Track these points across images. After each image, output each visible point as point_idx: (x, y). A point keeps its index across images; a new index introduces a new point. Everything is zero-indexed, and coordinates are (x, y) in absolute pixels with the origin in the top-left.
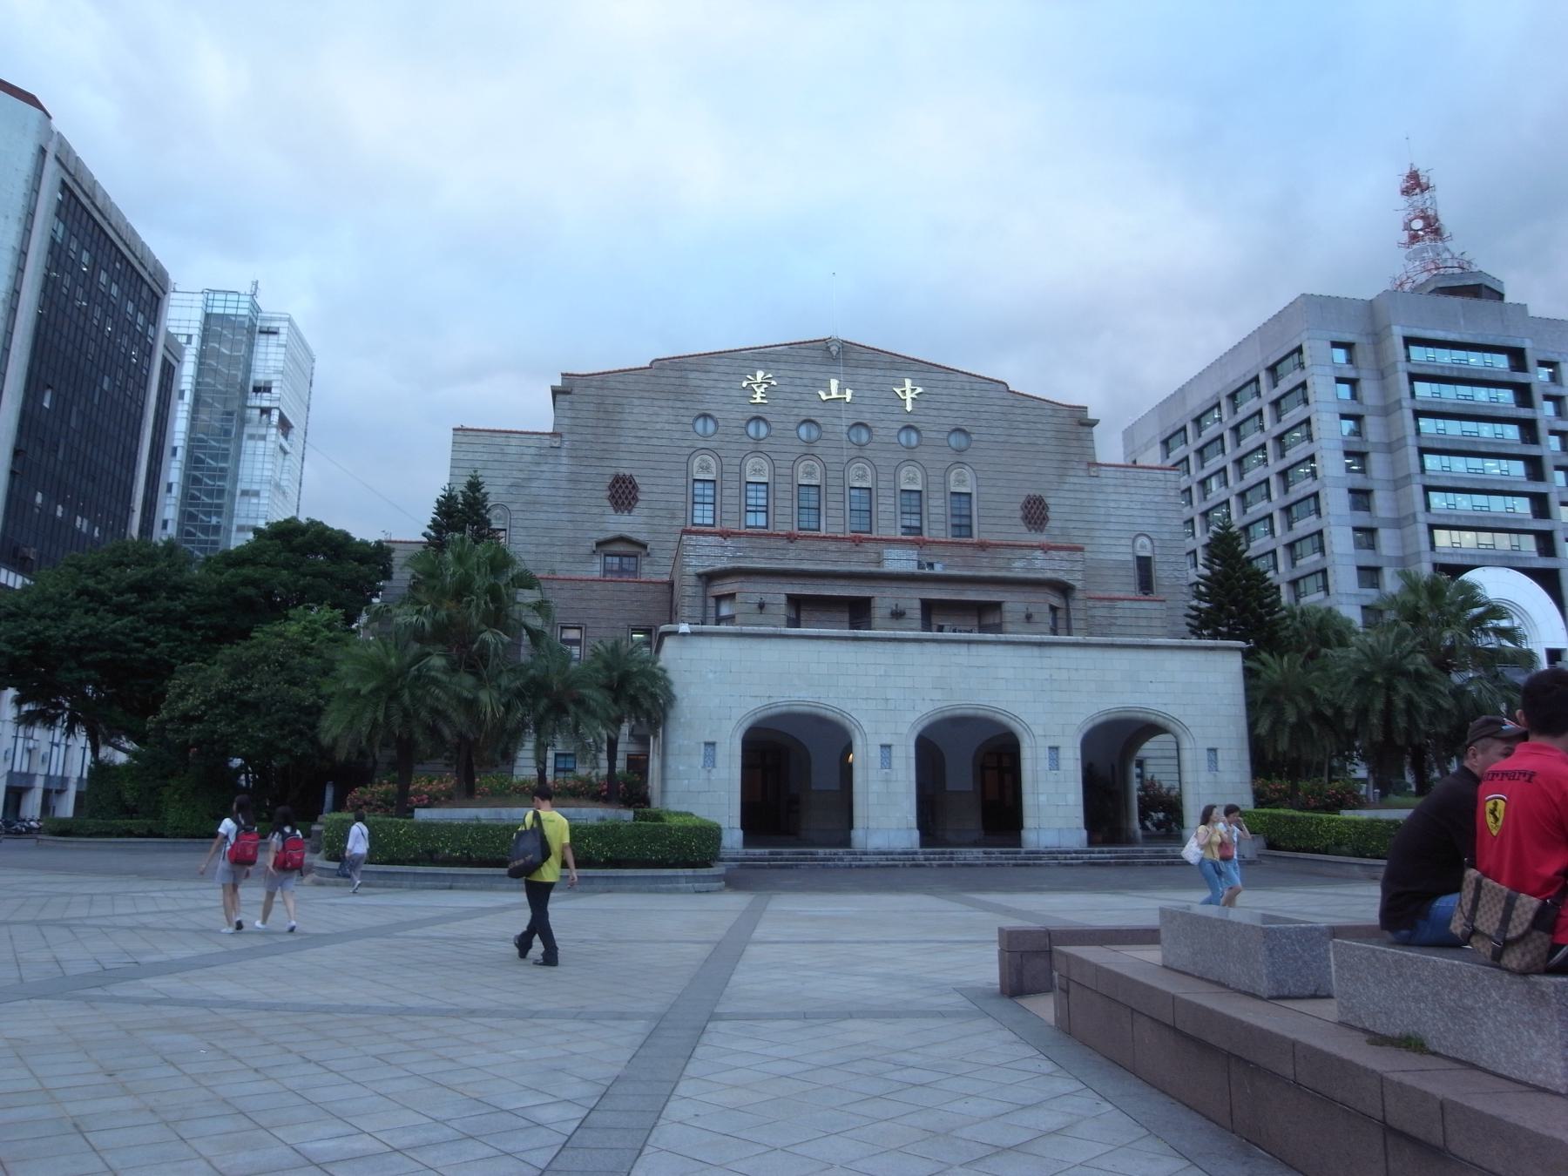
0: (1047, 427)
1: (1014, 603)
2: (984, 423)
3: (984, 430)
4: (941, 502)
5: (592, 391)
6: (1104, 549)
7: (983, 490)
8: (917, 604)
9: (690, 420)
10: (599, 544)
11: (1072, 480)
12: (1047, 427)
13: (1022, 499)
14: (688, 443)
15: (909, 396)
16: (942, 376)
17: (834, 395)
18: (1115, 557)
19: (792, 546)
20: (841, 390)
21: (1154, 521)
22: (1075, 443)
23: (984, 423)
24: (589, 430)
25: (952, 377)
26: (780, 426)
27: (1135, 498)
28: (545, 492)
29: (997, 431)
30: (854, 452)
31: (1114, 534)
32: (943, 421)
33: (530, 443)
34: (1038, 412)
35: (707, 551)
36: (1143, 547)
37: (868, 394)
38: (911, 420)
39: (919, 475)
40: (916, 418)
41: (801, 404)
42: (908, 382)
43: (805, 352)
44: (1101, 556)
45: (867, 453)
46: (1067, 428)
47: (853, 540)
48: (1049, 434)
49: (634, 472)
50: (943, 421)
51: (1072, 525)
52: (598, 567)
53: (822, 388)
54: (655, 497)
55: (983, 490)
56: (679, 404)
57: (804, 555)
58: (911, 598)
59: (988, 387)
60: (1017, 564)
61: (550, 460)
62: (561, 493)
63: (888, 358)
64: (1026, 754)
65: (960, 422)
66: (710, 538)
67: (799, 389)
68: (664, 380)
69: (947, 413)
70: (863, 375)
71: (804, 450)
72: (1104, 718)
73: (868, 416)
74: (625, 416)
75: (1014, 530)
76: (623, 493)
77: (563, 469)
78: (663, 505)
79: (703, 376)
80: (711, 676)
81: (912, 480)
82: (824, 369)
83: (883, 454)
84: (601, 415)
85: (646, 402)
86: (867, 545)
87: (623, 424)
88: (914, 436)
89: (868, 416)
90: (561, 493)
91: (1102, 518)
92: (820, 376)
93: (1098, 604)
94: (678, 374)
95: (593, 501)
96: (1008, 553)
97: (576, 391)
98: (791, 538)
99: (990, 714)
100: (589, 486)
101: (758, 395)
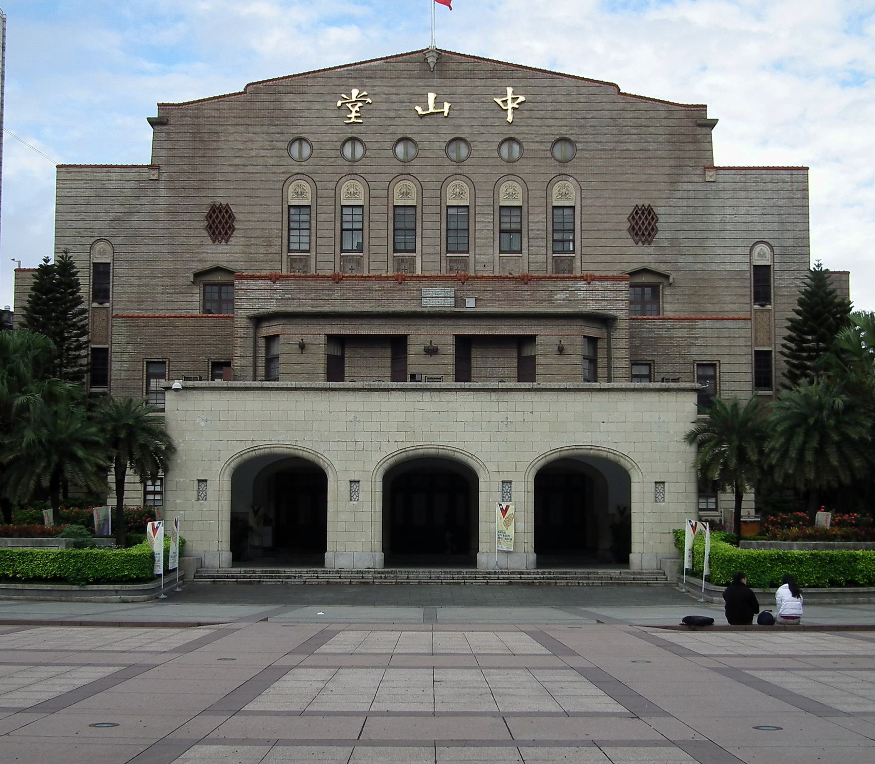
0: (661, 131)
1: (547, 336)
2: (590, 130)
3: (590, 138)
4: (542, 217)
5: (188, 120)
6: (718, 259)
7: (584, 202)
8: (451, 340)
9: (285, 145)
10: (197, 275)
11: (685, 186)
12: (661, 131)
13: (630, 210)
14: (283, 169)
15: (510, 105)
16: (547, 82)
17: (431, 110)
19: (337, 287)
20: (438, 103)
21: (776, 226)
22: (690, 146)
23: (590, 130)
24: (186, 161)
25: (557, 82)
26: (377, 146)
27: (755, 202)
28: (146, 225)
30: (451, 170)
31: (729, 243)
32: (547, 130)
33: (131, 176)
34: (652, 114)
35: (257, 294)
37: (466, 106)
38: (512, 132)
40: (518, 130)
41: (398, 121)
42: (510, 90)
43: (402, 66)
44: (714, 267)
45: (465, 170)
46: (682, 130)
47: (396, 278)
49: (230, 201)
50: (547, 130)
51: (681, 235)
52: (197, 297)
54: (251, 225)
55: (584, 202)
56: (273, 129)
57: (350, 295)
58: (445, 336)
59: (596, 90)
60: (560, 296)
61: (149, 193)
62: (160, 225)
63: (489, 66)
64: (482, 486)
65: (564, 131)
66: (260, 283)
67: (395, 106)
68: (258, 105)
69: (551, 122)
70: (462, 86)
71: (400, 170)
72: (556, 455)
73: (467, 130)
74: (221, 145)
75: (619, 243)
76: (220, 223)
77: (161, 201)
78: (258, 233)
79: (298, 98)
80: (203, 424)
81: (511, 196)
82: (420, 82)
83: (481, 170)
84: (198, 145)
85: (241, 129)
86: (410, 283)
87: (219, 153)
88: (516, 147)
89: (467, 130)
90: (160, 225)
91: (717, 227)
92: (418, 91)
94: (272, 97)
95: (192, 232)
96: (550, 286)
97: (172, 121)
98: (337, 279)
99: (450, 453)
100: (187, 217)
101: (353, 115)
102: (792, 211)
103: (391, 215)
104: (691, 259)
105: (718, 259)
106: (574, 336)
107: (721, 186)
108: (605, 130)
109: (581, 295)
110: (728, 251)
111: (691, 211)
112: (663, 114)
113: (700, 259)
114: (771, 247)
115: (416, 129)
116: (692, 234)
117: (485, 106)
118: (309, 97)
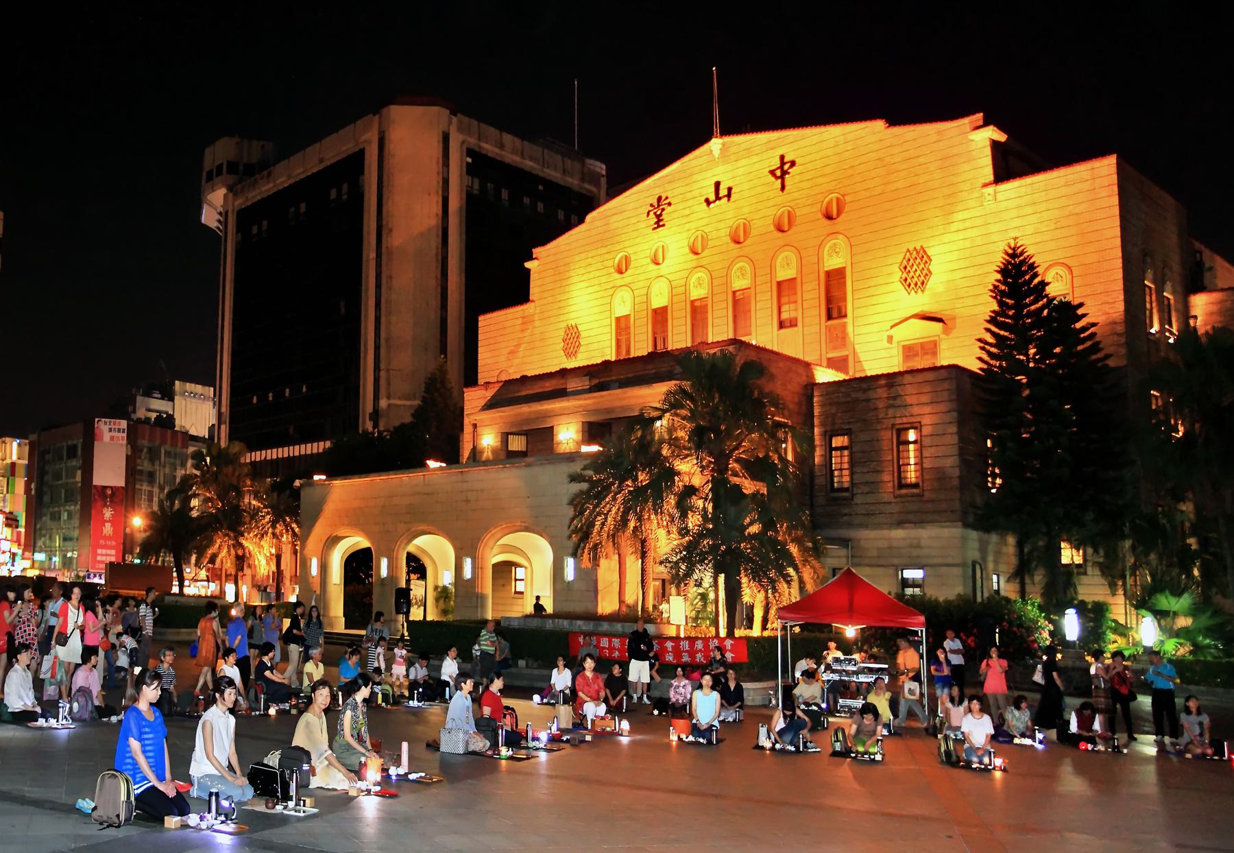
11: (961, 216)
41: (693, 217)
49: (577, 321)
68: (594, 232)
69: (821, 180)
114: (1069, 268)
115: (705, 221)
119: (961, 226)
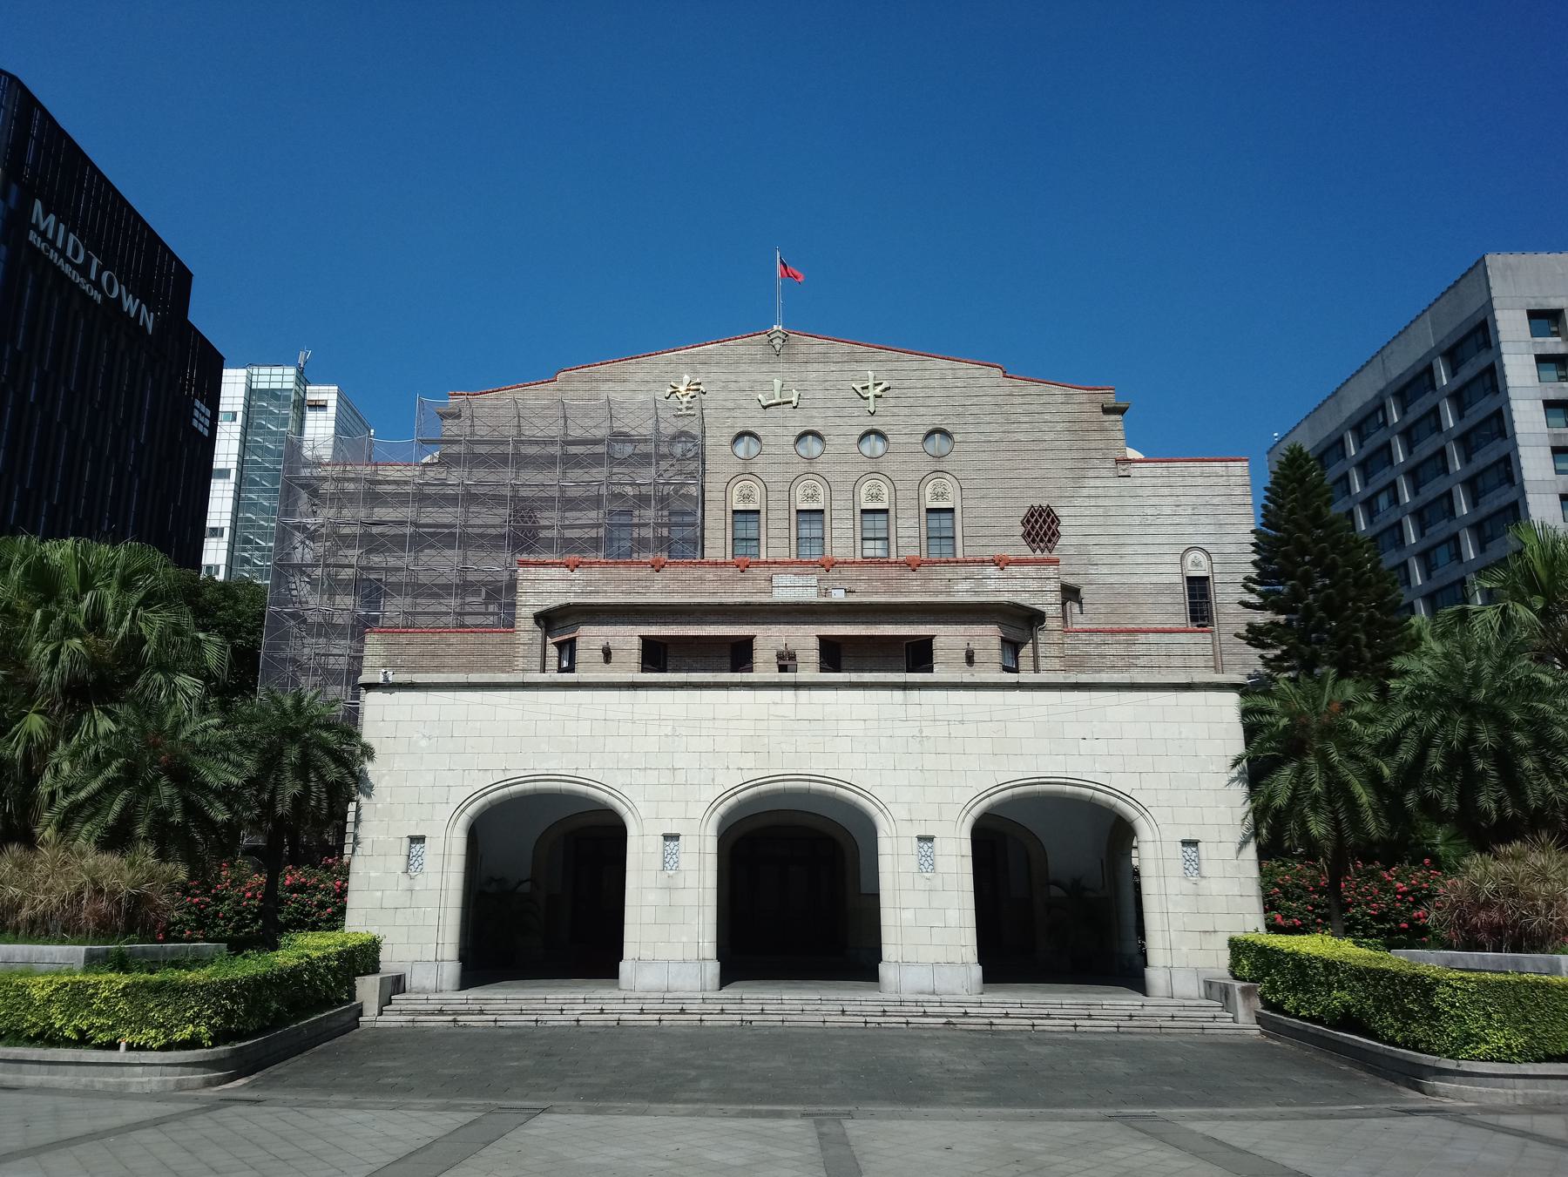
1: (948, 638)
3: (971, 428)
6: (1140, 570)
11: (1092, 483)
18: (1155, 579)
21: (1211, 529)
22: (1097, 436)
23: (970, 419)
29: (988, 429)
30: (802, 468)
31: (1151, 549)
34: (1045, 399)
36: (1196, 564)
37: (819, 395)
39: (885, 491)
40: (881, 420)
41: (737, 413)
44: (1135, 579)
45: (818, 468)
46: (1085, 417)
48: (1059, 427)
53: (762, 391)
59: (977, 373)
65: (938, 422)
69: (922, 410)
82: (765, 368)
91: (1137, 530)
93: (1109, 638)
96: (948, 572)
102: (1230, 510)
103: (729, 520)
104: (1105, 570)
105: (1140, 570)
106: (987, 636)
107: (1138, 482)
108: (988, 419)
109: (992, 585)
110: (1152, 559)
111: (1100, 511)
112: (1060, 399)
113: (1117, 569)
116: (1105, 540)
117: (842, 394)
118: (633, 386)
119: (1093, 492)
